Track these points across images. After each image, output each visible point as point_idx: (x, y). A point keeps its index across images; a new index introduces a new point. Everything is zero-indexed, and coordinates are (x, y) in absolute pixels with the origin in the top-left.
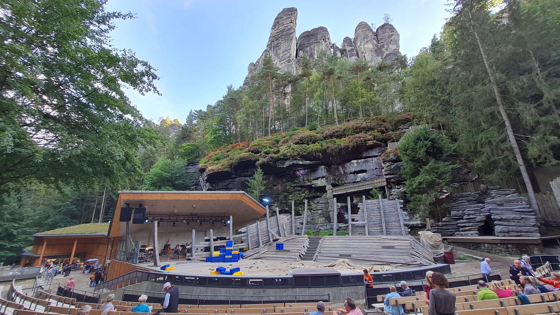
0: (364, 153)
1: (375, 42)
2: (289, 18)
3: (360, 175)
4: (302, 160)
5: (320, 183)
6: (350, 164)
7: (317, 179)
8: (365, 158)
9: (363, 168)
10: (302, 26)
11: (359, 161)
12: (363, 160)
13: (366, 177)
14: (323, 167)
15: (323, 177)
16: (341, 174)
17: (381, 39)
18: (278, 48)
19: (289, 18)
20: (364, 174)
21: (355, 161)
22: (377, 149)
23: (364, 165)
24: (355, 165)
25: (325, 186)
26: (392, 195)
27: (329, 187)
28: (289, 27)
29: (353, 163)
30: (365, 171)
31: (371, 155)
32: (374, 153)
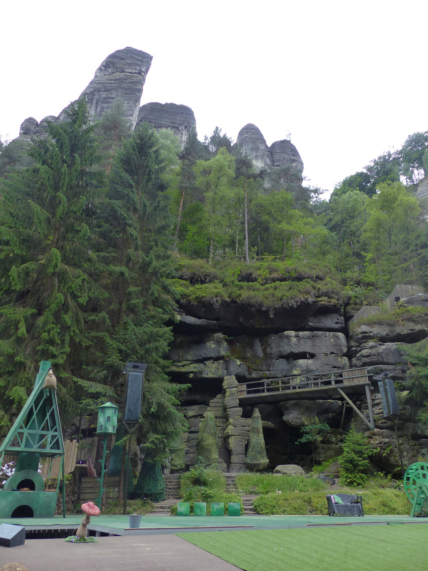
0: (311, 319)
1: (268, 161)
2: (138, 65)
3: (301, 361)
4: (180, 313)
5: (211, 370)
6: (281, 337)
7: (202, 361)
8: (312, 329)
9: (307, 348)
10: (155, 90)
11: (301, 333)
12: (307, 333)
13: (313, 367)
14: (220, 335)
15: (217, 359)
16: (255, 356)
17: (278, 161)
18: (106, 105)
19: (138, 65)
20: (310, 361)
21: (292, 333)
22: (334, 315)
23: (309, 343)
24: (294, 340)
25: (221, 380)
26: (378, 404)
27: (229, 381)
28: (134, 79)
29: (288, 337)
30: (312, 356)
31: (322, 325)
32: (330, 321)
